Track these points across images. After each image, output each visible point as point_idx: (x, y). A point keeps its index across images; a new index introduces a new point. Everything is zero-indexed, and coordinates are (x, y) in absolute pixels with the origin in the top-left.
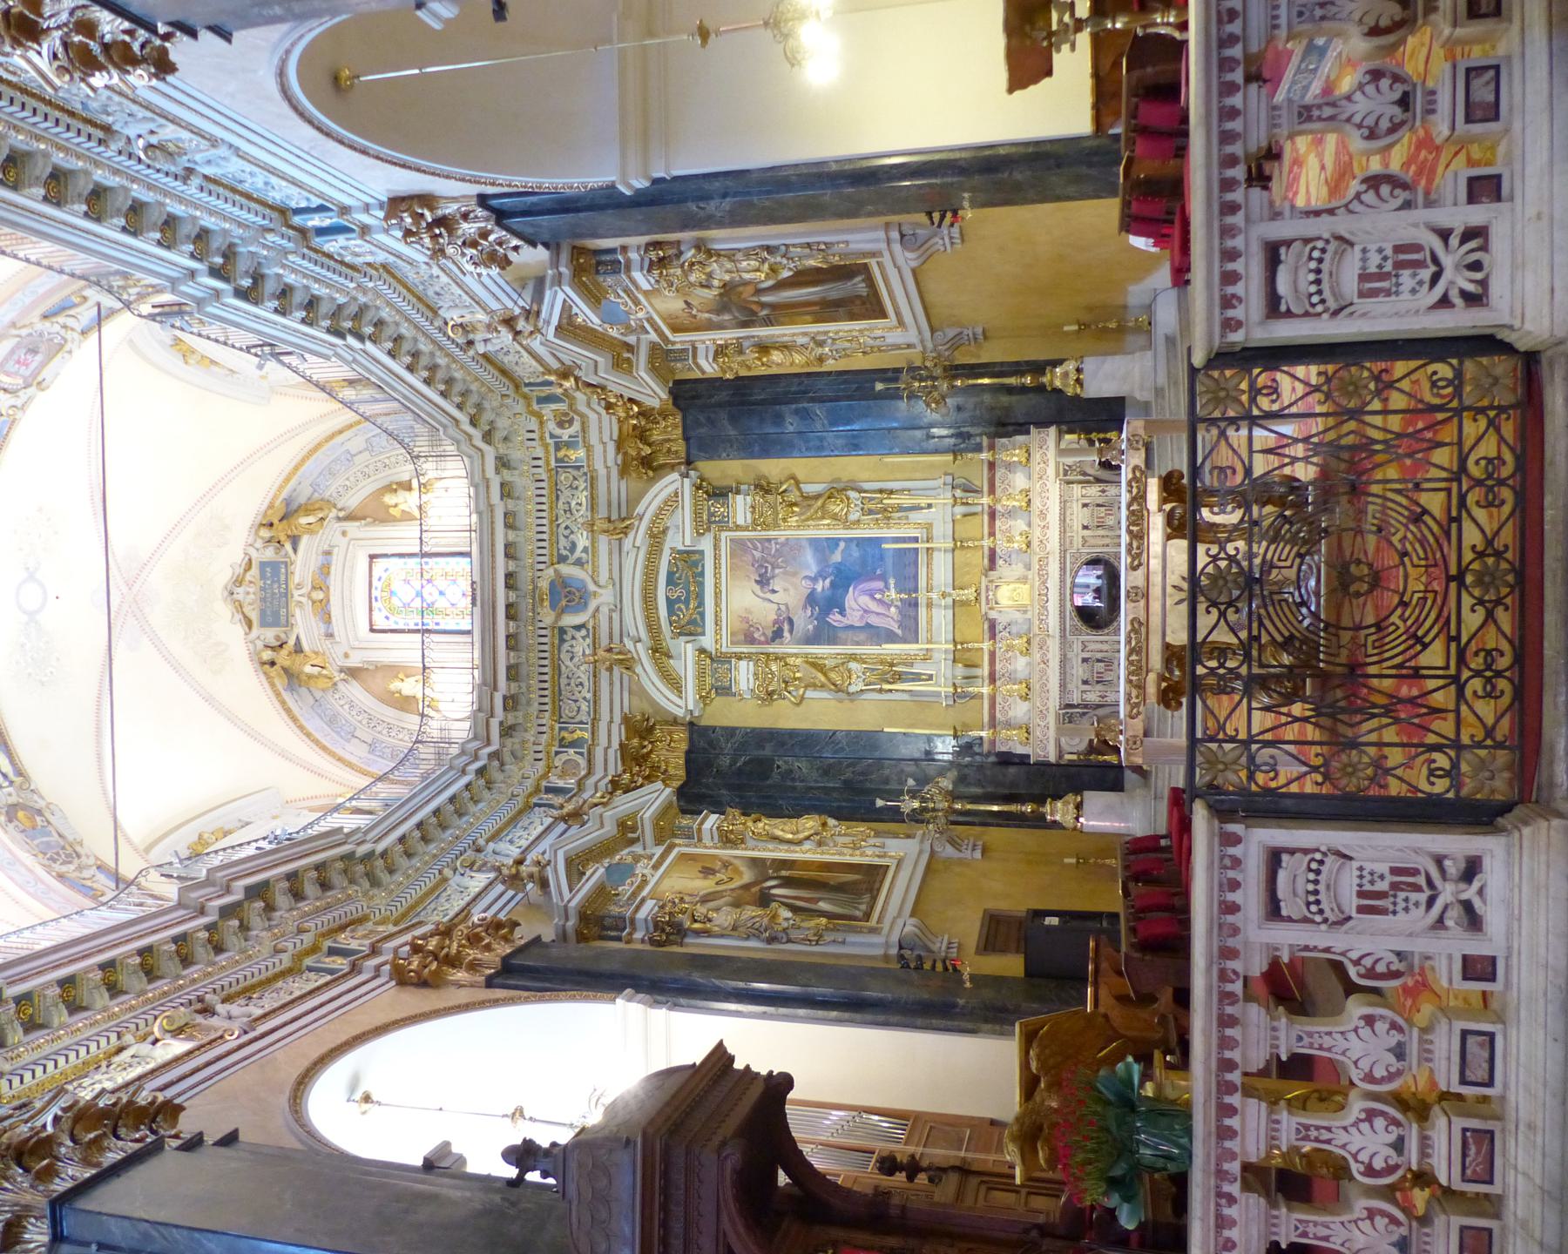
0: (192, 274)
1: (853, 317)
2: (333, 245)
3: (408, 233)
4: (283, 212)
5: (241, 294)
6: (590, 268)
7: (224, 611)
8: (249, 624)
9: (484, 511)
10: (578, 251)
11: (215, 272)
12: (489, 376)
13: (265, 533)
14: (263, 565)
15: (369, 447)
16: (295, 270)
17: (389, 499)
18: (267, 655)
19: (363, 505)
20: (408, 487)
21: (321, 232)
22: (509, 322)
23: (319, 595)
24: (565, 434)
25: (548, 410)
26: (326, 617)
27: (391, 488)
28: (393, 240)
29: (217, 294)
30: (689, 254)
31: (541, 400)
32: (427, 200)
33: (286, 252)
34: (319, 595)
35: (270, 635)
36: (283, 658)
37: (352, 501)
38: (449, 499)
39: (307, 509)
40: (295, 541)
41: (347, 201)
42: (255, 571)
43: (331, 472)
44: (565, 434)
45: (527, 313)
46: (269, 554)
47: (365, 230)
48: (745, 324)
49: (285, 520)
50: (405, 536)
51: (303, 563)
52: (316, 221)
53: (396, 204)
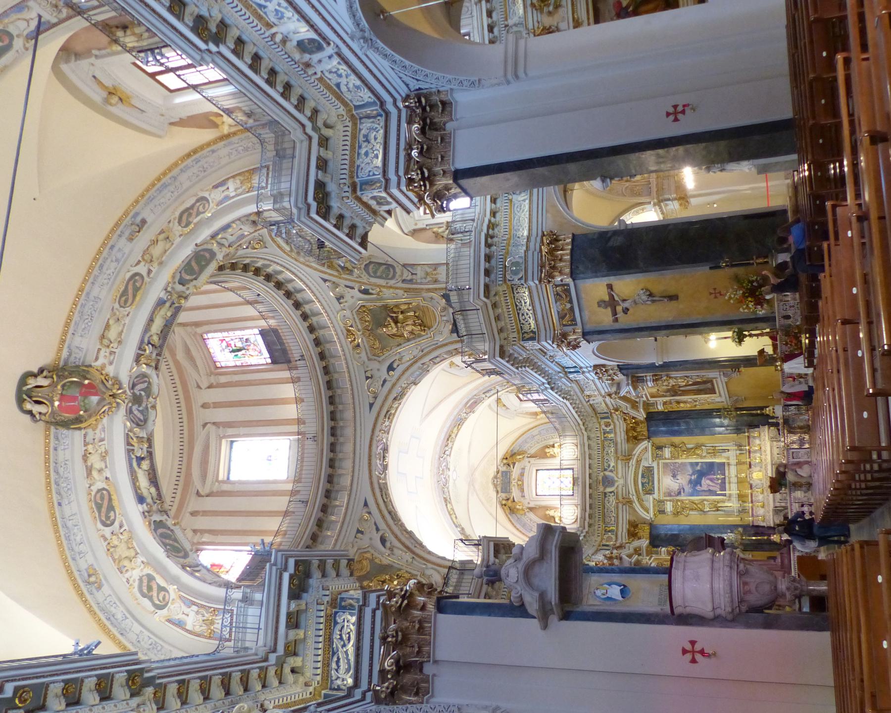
0: (544, 383)
1: (706, 394)
2: (571, 376)
3: (596, 373)
4: (564, 368)
5: (552, 389)
6: (636, 381)
7: (491, 487)
8: (497, 492)
9: (583, 454)
10: (633, 377)
11: (549, 383)
12: (590, 410)
13: (505, 461)
14: (503, 472)
15: (540, 433)
16: (563, 383)
17: (547, 450)
18: (504, 502)
19: (535, 453)
20: (553, 446)
21: (570, 372)
22: (610, 395)
23: (520, 483)
24: (608, 429)
25: (603, 421)
26: (522, 491)
27: (547, 447)
28: (592, 376)
29: (546, 388)
30: (665, 378)
31: (602, 418)
32: (604, 366)
33: (561, 377)
34: (520, 483)
35: (504, 495)
36: (509, 503)
37: (532, 451)
38: (568, 451)
39: (519, 455)
40: (514, 464)
41: (582, 365)
42: (500, 474)
43: (526, 442)
44: (608, 429)
45: (616, 393)
46: (505, 469)
47: (583, 372)
48: (673, 396)
49: (511, 458)
50: (555, 463)
51: (515, 472)
52: (572, 370)
53: (596, 367)
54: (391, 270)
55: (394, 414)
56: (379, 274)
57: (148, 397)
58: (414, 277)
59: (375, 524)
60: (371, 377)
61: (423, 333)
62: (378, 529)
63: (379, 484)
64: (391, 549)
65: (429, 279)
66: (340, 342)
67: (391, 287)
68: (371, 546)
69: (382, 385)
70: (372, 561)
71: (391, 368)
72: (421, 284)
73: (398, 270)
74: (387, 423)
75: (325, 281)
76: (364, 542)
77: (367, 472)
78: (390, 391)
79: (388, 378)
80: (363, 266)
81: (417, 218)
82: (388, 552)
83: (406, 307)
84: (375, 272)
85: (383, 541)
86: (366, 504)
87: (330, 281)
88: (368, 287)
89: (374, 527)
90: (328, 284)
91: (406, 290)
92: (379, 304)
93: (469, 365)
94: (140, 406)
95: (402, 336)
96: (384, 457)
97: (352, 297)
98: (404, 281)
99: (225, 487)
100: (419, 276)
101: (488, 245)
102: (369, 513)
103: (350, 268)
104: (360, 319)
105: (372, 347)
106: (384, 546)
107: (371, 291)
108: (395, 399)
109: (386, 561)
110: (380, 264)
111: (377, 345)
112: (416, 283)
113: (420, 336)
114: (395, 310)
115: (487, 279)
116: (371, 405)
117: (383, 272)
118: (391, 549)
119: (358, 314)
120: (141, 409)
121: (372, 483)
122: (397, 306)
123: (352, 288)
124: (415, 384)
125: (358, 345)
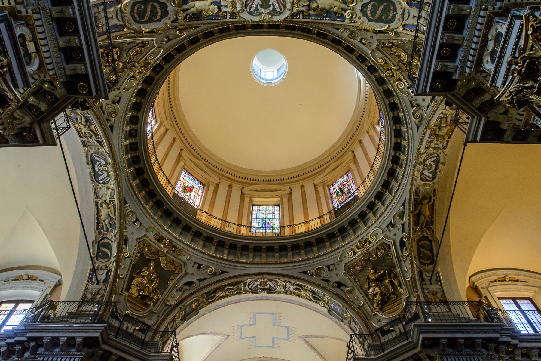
54: (429, 262)
55: (299, 295)
56: (422, 250)
57: (269, 13)
58: (428, 282)
59: (205, 279)
60: (329, 270)
61: (375, 305)
62: (200, 280)
63: (240, 283)
64: (181, 290)
65: (430, 296)
66: (355, 239)
67: (412, 262)
68: (186, 274)
69: (323, 280)
70: (172, 272)
71: (340, 285)
72: (423, 290)
73: (431, 267)
74: (292, 288)
75: (404, 205)
76: (191, 269)
77: (247, 272)
78: (318, 286)
79: (331, 283)
80: (425, 234)
81: (489, 289)
82: (179, 287)
83: (396, 283)
84: (423, 246)
85: (190, 284)
86: (223, 272)
87: (404, 208)
88: (407, 244)
89: (202, 278)
90: (402, 208)
91: (413, 279)
92: (395, 261)
93: (349, 349)
94: (261, 6)
95: (369, 287)
96: (264, 290)
97: (395, 235)
98: (421, 273)
99: (247, 200)
100: (429, 286)
101: (486, 342)
102: (215, 274)
103: (421, 222)
104: (377, 248)
105: (355, 265)
106: (185, 284)
107: (405, 248)
108: (313, 292)
109: (171, 284)
110: (431, 250)
111: (358, 269)
112: (422, 286)
113: (372, 303)
114: (392, 276)
115: (444, 341)
116: (306, 273)
117: (425, 254)
118: (181, 290)
119: (381, 245)
120: (259, 8)
121: (240, 276)
122: (396, 277)
123: (403, 231)
124: (329, 311)
125: (355, 253)
